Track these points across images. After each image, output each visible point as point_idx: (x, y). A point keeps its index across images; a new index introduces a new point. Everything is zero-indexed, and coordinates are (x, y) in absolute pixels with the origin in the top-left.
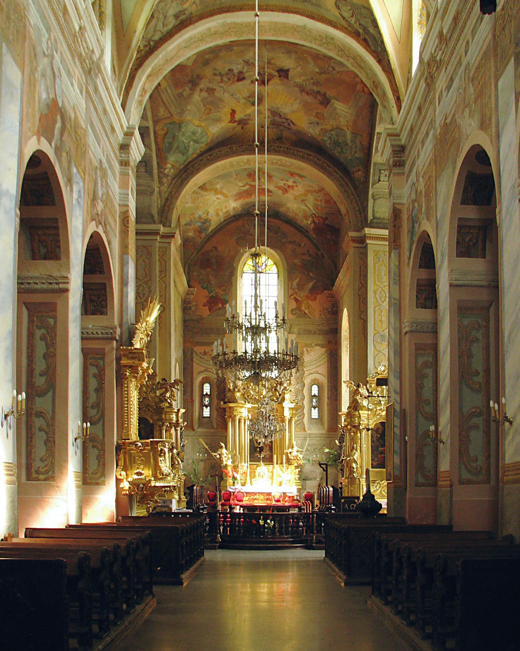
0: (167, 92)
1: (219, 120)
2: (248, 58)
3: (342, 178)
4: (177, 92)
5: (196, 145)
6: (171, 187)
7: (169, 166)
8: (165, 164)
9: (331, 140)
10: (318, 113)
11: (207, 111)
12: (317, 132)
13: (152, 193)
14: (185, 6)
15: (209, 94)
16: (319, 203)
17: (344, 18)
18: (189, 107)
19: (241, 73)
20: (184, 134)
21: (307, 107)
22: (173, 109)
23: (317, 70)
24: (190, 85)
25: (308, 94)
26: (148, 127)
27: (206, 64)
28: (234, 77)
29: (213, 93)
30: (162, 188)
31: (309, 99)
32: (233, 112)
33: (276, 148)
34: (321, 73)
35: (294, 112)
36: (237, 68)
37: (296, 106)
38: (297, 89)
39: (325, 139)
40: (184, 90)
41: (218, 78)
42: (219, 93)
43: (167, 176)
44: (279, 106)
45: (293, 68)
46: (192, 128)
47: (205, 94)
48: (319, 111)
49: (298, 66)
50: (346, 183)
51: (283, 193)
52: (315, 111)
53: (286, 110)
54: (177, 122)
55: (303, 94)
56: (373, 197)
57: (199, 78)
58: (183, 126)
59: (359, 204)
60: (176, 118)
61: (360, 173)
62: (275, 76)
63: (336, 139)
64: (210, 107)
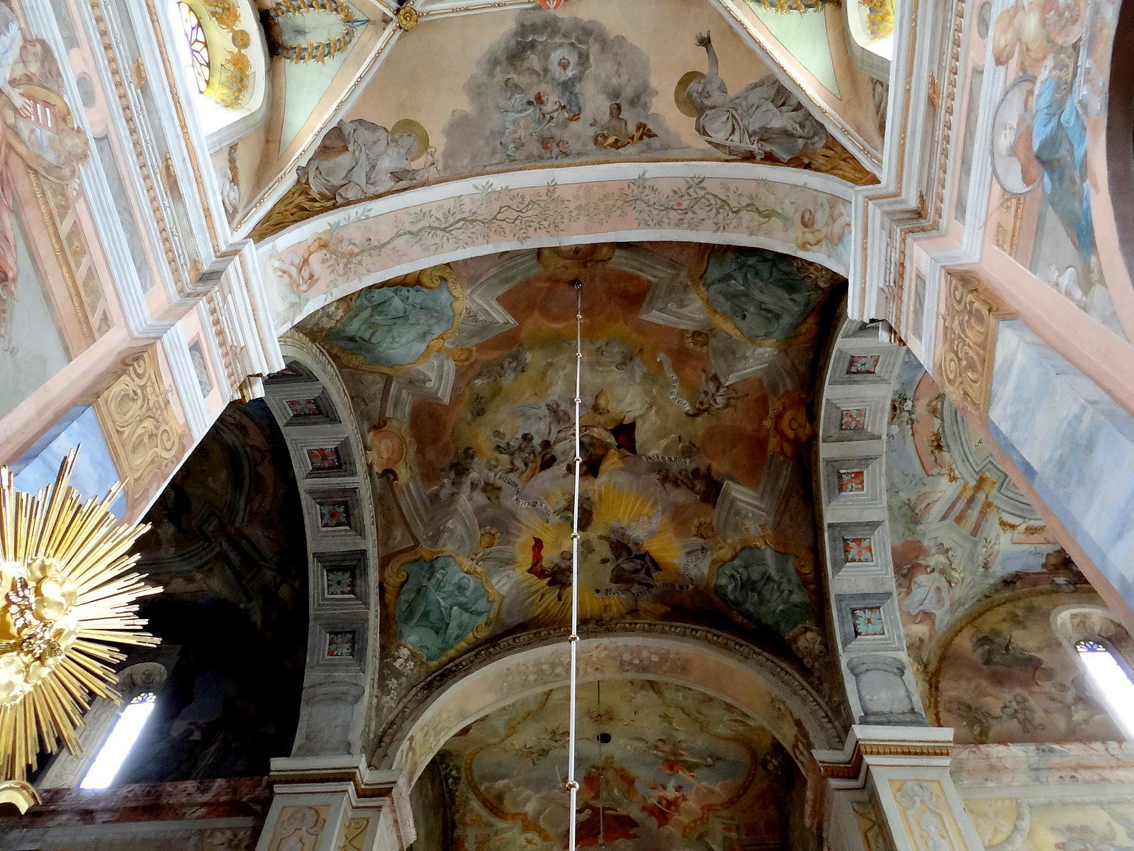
0: (409, 491)
1: (510, 562)
2: (555, 398)
3: (772, 662)
4: (429, 492)
5: (466, 616)
6: (405, 700)
7: (405, 652)
8: (397, 648)
9: (735, 580)
10: (700, 524)
11: (487, 539)
12: (706, 571)
13: (357, 699)
14: (416, 165)
15: (489, 499)
16: (734, 835)
17: (717, 146)
18: (449, 524)
19: (546, 444)
20: (439, 588)
21: (679, 518)
22: (420, 530)
23: (687, 408)
24: (452, 474)
25: (676, 484)
26: (364, 552)
27: (479, 414)
28: (535, 457)
29: (497, 497)
30: (385, 699)
31: (680, 496)
32: (538, 544)
33: (627, 626)
34: (694, 416)
35: (652, 534)
36: (539, 429)
37: (657, 521)
38: (655, 477)
39: (724, 581)
40: (442, 486)
41: (505, 458)
42: (508, 500)
43: (398, 674)
44: (624, 524)
45: (641, 416)
46: (455, 575)
47: (480, 498)
48: (702, 519)
49: (650, 407)
50: (782, 669)
51: (660, 825)
52: (696, 522)
53: (637, 532)
54: (427, 557)
55: (668, 486)
56: (852, 670)
57: (469, 454)
58: (438, 565)
59: (823, 704)
60: (425, 550)
61: (809, 635)
62: (606, 447)
63: (745, 575)
64: (494, 531)
